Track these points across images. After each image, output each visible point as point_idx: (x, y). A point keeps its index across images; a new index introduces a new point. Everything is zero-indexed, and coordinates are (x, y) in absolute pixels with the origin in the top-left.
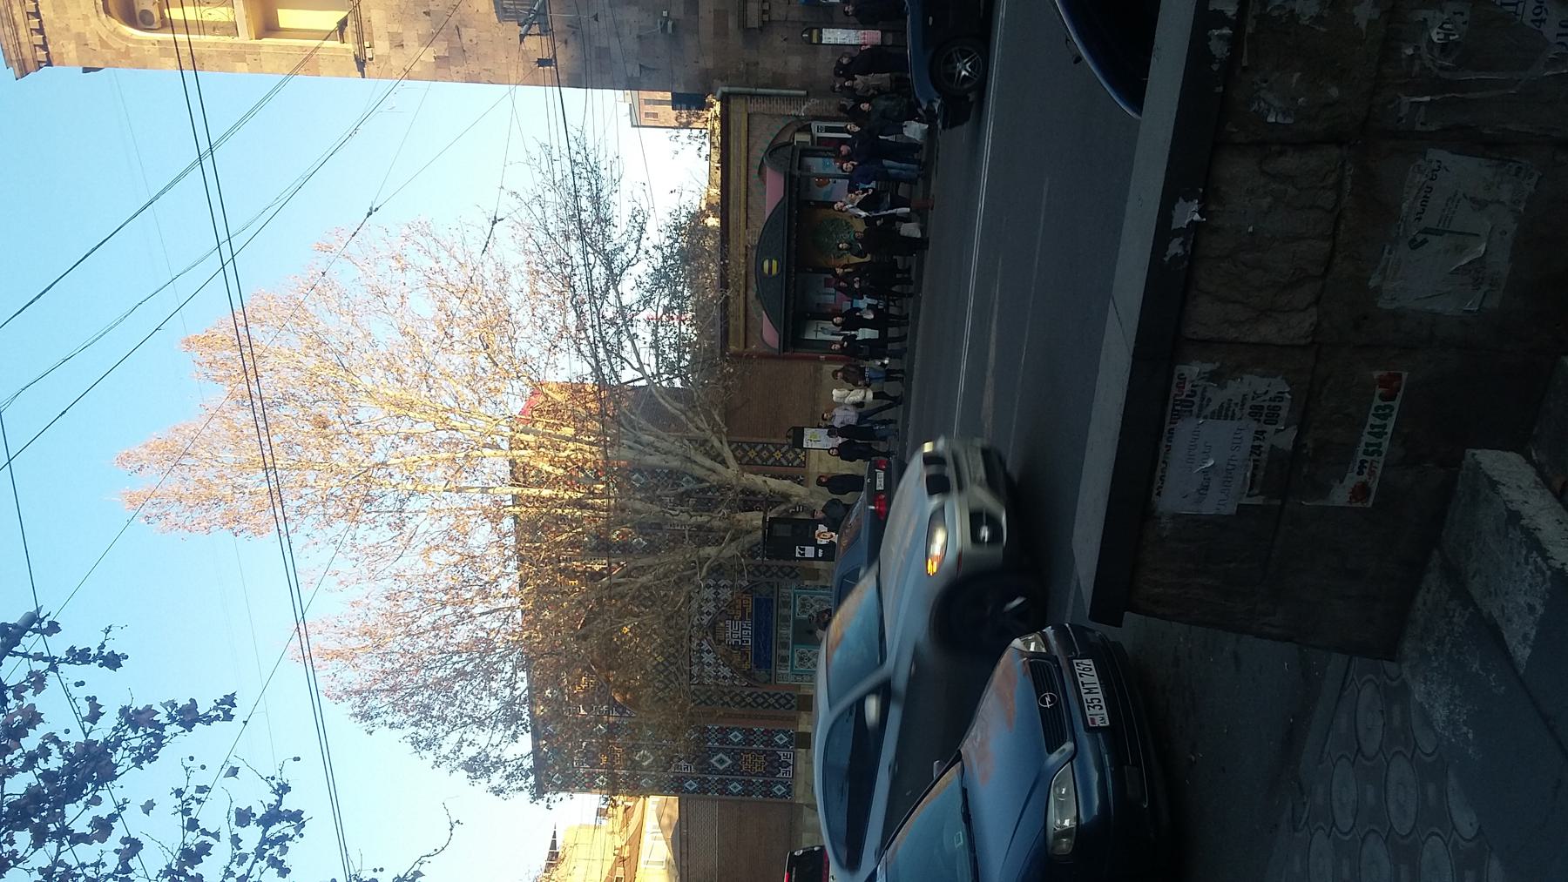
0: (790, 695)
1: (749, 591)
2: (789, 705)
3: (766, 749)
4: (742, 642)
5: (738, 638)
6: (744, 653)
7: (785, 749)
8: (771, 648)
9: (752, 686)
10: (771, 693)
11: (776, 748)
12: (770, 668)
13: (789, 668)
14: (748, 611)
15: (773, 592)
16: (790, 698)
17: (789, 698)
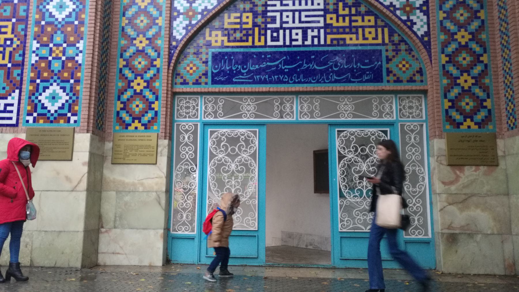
0: (154, 120)
1: (396, 38)
2: (128, 119)
3: (27, 68)
4: (277, 30)
5: (282, 22)
6: (248, 34)
7: (26, 107)
8: (265, 82)
9: (171, 48)
10: (157, 84)
11: (27, 87)
12: (214, 82)
13: (211, 119)
14: (351, 39)
15: (398, 81)
16: (145, 119)
17: (145, 119)
